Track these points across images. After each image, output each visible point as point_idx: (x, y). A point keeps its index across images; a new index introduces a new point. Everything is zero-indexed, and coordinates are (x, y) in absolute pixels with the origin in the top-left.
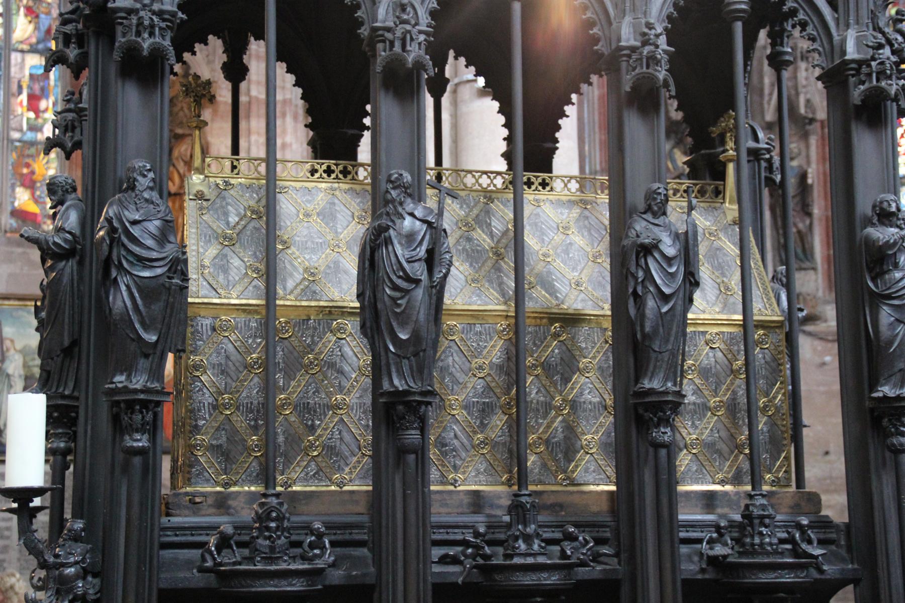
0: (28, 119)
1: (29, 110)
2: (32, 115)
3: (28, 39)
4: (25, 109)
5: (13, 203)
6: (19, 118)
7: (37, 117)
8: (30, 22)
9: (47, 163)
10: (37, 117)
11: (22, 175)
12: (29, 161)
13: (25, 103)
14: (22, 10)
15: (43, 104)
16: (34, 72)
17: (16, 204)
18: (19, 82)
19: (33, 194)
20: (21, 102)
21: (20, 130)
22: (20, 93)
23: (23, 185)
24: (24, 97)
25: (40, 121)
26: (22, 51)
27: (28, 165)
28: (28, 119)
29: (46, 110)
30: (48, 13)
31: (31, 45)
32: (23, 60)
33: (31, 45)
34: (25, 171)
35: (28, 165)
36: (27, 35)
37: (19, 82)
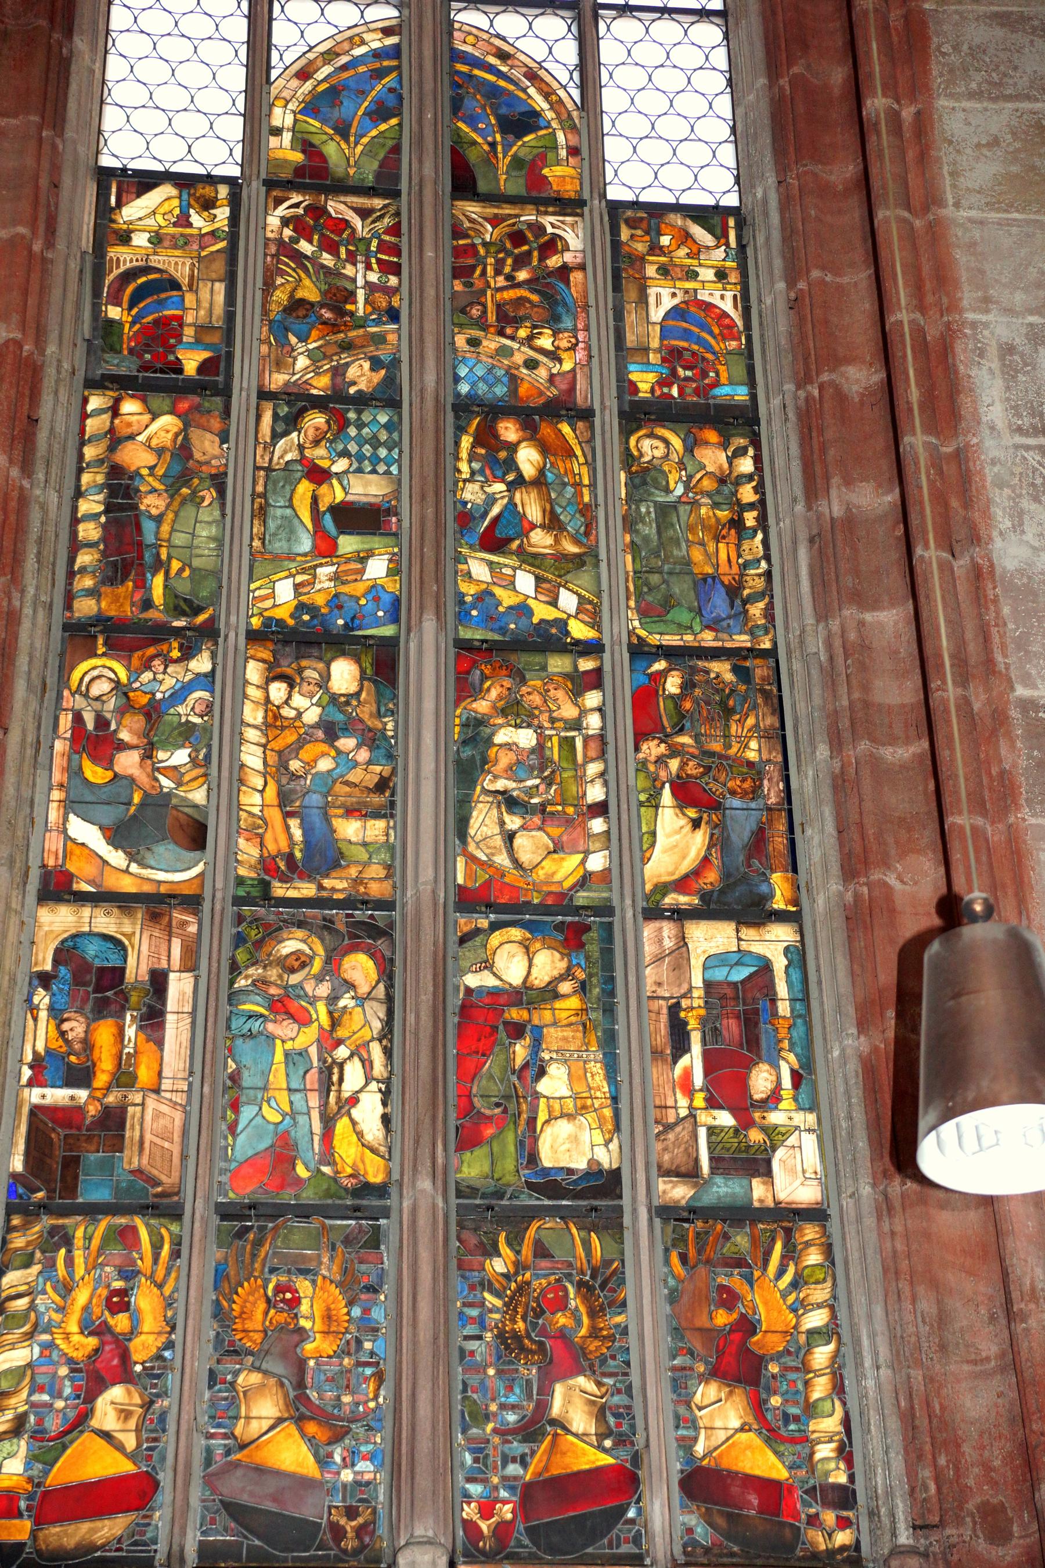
0: (712, 1130)
1: (712, 1103)
2: (725, 1119)
3: (696, 873)
4: (699, 1101)
5: (687, 1444)
6: (682, 1132)
7: (745, 1122)
8: (696, 824)
9: (795, 1285)
10: (745, 1122)
11: (707, 1333)
12: (735, 1281)
13: (698, 1079)
14: (667, 796)
15: (761, 1081)
16: (719, 974)
17: (700, 1449)
18: (674, 1009)
19: (758, 1407)
20: (688, 1074)
21: (690, 1173)
22: (680, 1044)
23: (716, 1373)
24: (694, 1060)
25: (755, 1136)
26: (679, 915)
27: (729, 1299)
28: (712, 1130)
29: (774, 1098)
30: (755, 792)
31: (705, 897)
32: (682, 941)
33: (705, 897)
34: (722, 1318)
35: (729, 1299)
36: (687, 865)
37: (674, 1009)
